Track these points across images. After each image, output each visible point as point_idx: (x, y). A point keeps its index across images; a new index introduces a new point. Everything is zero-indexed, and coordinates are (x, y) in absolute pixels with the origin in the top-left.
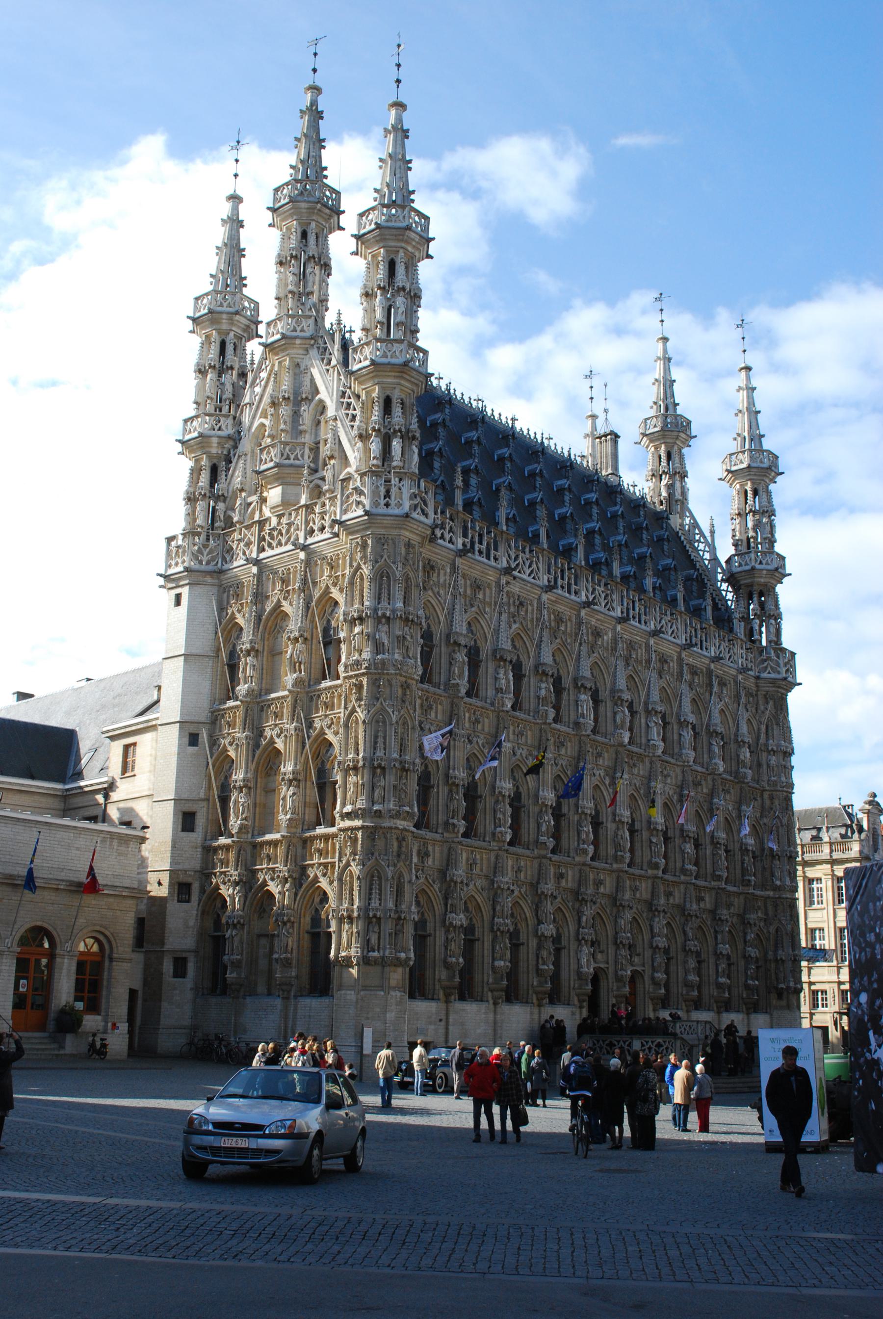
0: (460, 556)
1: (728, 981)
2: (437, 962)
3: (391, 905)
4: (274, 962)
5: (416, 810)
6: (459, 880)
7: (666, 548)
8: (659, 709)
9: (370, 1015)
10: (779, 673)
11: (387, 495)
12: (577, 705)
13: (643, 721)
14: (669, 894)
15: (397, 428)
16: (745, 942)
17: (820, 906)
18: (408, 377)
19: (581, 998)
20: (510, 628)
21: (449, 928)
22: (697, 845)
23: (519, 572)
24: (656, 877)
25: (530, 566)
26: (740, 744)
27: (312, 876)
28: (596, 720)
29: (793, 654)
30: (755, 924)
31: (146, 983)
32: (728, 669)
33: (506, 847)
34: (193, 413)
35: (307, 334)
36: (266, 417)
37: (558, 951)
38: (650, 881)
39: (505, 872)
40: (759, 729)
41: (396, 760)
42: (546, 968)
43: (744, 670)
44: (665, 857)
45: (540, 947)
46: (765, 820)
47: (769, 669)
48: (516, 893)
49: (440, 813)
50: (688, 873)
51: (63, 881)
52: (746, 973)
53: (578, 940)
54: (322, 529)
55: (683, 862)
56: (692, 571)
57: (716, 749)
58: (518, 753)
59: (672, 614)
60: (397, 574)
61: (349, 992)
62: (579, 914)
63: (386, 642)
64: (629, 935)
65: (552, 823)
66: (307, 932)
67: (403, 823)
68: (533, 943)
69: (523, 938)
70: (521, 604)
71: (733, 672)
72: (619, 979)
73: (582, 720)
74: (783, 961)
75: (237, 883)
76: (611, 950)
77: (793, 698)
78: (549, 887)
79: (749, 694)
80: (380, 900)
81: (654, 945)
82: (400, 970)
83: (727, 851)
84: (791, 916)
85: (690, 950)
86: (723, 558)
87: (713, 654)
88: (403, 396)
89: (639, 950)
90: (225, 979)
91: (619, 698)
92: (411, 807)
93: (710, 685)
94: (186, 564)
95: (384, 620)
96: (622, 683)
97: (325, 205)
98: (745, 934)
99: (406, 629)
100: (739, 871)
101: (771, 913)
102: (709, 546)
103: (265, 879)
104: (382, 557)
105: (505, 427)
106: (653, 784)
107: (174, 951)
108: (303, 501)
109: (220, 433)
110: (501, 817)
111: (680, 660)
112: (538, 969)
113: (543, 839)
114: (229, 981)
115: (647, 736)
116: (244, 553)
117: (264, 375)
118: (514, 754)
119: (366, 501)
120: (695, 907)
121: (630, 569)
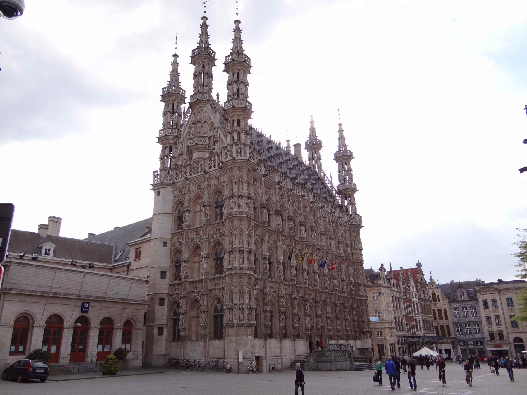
3: (247, 302)
4: (199, 328)
14: (330, 298)
16: (353, 315)
35: (207, 99)
41: (247, 248)
43: (347, 222)
45: (294, 318)
53: (305, 315)
54: (214, 166)
57: (341, 248)
68: (291, 316)
69: (287, 315)
75: (184, 297)
77: (361, 231)
78: (295, 296)
82: (251, 328)
90: (179, 335)
96: (313, 224)
97: (211, 56)
98: (353, 312)
100: (349, 290)
101: (359, 305)
105: (267, 138)
111: (329, 217)
112: (293, 326)
113: (293, 278)
117: (189, 114)
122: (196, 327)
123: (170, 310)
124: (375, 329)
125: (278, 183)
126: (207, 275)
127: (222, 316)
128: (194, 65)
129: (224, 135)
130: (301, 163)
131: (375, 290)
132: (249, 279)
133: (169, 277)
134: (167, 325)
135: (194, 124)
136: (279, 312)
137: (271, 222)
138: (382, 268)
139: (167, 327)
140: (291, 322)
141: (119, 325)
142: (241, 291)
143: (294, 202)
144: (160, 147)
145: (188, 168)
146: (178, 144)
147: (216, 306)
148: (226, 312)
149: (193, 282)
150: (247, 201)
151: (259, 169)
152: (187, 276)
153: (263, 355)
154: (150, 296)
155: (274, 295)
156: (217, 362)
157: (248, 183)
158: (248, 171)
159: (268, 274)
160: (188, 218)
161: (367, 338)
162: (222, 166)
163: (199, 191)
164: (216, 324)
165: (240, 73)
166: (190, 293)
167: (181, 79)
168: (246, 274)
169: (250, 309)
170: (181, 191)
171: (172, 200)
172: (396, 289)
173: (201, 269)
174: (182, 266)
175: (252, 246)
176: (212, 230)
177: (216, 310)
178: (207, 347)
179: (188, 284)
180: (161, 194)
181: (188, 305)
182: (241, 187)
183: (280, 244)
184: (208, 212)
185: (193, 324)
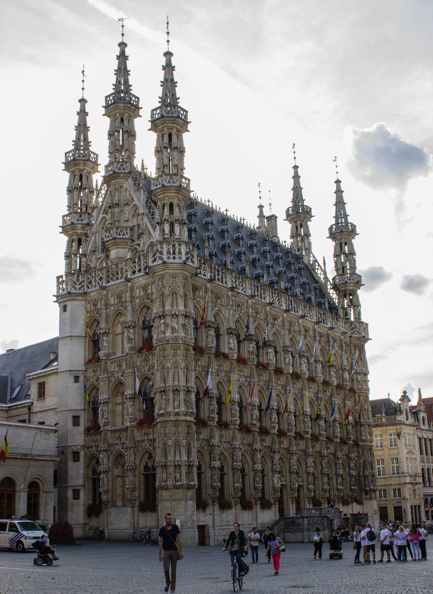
0: (209, 282)
2: (208, 485)
3: (186, 458)
4: (126, 490)
5: (195, 411)
6: (216, 445)
7: (302, 273)
8: (306, 355)
10: (360, 334)
11: (174, 253)
13: (298, 361)
14: (313, 447)
15: (177, 219)
16: (349, 468)
17: (381, 448)
19: (275, 499)
20: (234, 317)
21: (212, 468)
25: (242, 286)
26: (344, 370)
27: (144, 446)
29: (367, 324)
32: (337, 334)
33: (238, 427)
34: (67, 213)
36: (107, 214)
40: (352, 363)
41: (184, 386)
43: (344, 333)
45: (255, 476)
46: (357, 408)
48: (243, 449)
52: (350, 483)
53: (273, 471)
54: (140, 271)
55: (320, 430)
56: (316, 285)
57: (333, 373)
58: (241, 380)
59: (309, 307)
60: (181, 293)
62: (272, 459)
63: (177, 327)
67: (189, 417)
68: (252, 474)
69: (246, 471)
70: (239, 305)
71: (339, 334)
72: (292, 489)
76: (288, 475)
77: (368, 346)
78: (258, 446)
79: (347, 345)
80: (180, 456)
82: (191, 490)
83: (339, 424)
86: (330, 277)
87: (329, 326)
88: (179, 202)
89: (301, 475)
91: (287, 350)
92: (193, 410)
93: (329, 342)
94: (69, 290)
95: (175, 316)
96: (288, 343)
98: (349, 464)
99: (186, 320)
100: (345, 434)
102: (323, 271)
104: (173, 284)
105: (222, 214)
106: (304, 392)
107: (72, 486)
108: (129, 257)
109: (82, 222)
111: (314, 330)
112: (254, 487)
113: (254, 422)
117: (103, 192)
118: (239, 381)
119: (165, 257)
120: (326, 452)
121: (289, 285)
122: (121, 489)
123: (87, 467)
124: (391, 485)
125: (232, 289)
127: (154, 475)
128: (110, 117)
129: (152, 225)
130: (276, 246)
131: (392, 430)
133: (85, 424)
134: (84, 486)
135: (110, 207)
137: (222, 344)
138: (405, 398)
139: (84, 489)
140: (251, 481)
142: (177, 444)
143: (257, 313)
144: (65, 239)
146: (90, 236)
147: (146, 463)
148: (159, 471)
149: (116, 431)
150: (183, 322)
151: (203, 272)
153: (210, 523)
155: (226, 445)
157: (185, 295)
158: (186, 278)
159: (217, 420)
160: (105, 344)
161: (371, 499)
162: (148, 271)
167: (91, 136)
168: (183, 420)
169: (190, 466)
170: (95, 305)
172: (426, 427)
174: (100, 409)
175: (192, 384)
176: (139, 360)
177: (146, 468)
179: (109, 433)
180: (68, 309)
181: (110, 462)
182: (175, 301)
184: (132, 337)
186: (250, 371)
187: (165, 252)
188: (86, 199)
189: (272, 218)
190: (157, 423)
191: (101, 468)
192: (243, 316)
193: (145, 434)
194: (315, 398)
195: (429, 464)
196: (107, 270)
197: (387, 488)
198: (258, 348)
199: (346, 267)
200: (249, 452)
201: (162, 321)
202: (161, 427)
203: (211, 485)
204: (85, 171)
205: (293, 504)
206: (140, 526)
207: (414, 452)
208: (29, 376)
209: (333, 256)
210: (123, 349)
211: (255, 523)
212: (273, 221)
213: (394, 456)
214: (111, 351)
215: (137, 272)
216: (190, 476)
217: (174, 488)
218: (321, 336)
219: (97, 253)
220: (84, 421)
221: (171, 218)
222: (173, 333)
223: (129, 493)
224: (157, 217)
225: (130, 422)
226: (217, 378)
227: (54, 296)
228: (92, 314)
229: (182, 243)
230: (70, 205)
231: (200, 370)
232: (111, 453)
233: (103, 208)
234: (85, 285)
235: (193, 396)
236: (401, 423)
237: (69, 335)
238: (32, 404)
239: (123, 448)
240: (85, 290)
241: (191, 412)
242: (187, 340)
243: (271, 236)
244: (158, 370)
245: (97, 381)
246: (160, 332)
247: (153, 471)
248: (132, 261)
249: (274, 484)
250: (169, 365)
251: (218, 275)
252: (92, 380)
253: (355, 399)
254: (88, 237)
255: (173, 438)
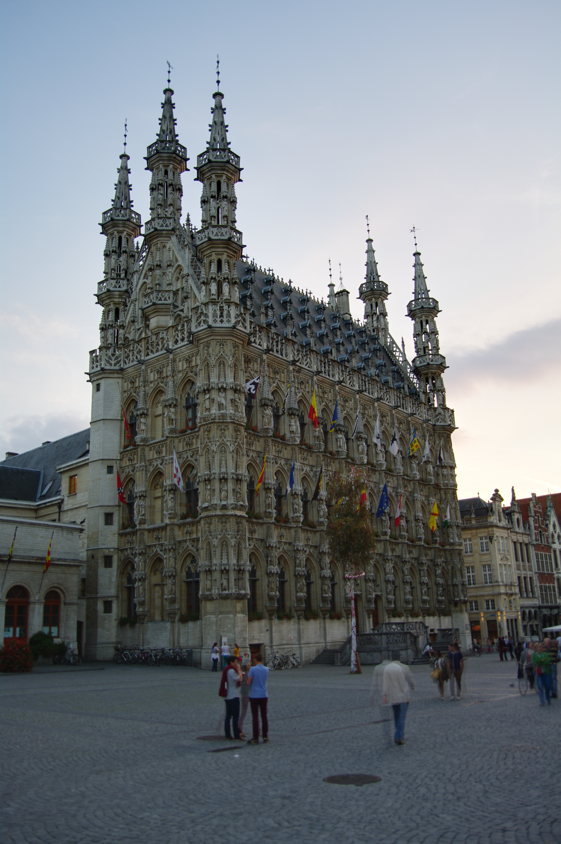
0: (266, 353)
1: (428, 598)
3: (235, 561)
4: (165, 601)
5: (247, 504)
6: (274, 545)
7: (378, 354)
9: (225, 629)
10: (445, 422)
11: (222, 316)
12: (337, 441)
13: (374, 450)
14: (393, 550)
15: (226, 276)
16: (436, 575)
17: (471, 554)
18: (231, 248)
20: (297, 395)
21: (269, 574)
22: (407, 522)
23: (300, 363)
24: (386, 540)
27: (185, 547)
28: (348, 450)
30: (441, 565)
31: (88, 617)
33: (301, 525)
35: (170, 228)
36: (147, 279)
37: (333, 585)
38: (382, 543)
39: (301, 540)
41: (233, 473)
42: (327, 595)
43: (427, 421)
44: (390, 529)
46: (443, 506)
47: (440, 420)
48: (308, 552)
49: (261, 506)
50: (403, 537)
51: (33, 557)
52: (437, 593)
54: (183, 340)
56: (394, 367)
57: (415, 466)
58: (305, 469)
60: (230, 362)
61: (211, 616)
63: (224, 403)
64: (373, 574)
65: (326, 510)
66: (184, 582)
67: (239, 512)
68: (319, 582)
69: (313, 579)
72: (369, 601)
73: (340, 449)
74: (456, 585)
75: (140, 554)
80: (228, 559)
81: (387, 579)
82: (242, 602)
83: (423, 524)
84: (460, 559)
85: (406, 581)
86: (410, 360)
87: (410, 412)
90: (135, 613)
92: (244, 501)
93: (409, 429)
94: (103, 366)
95: (222, 390)
96: (361, 429)
97: (178, 155)
98: (436, 571)
99: (236, 395)
101: (449, 559)
103: (157, 551)
108: (170, 325)
110: (297, 507)
111: (392, 415)
112: (322, 597)
113: (322, 519)
114: (138, 613)
115: (376, 459)
116: (137, 358)
117: (144, 254)
118: (303, 470)
120: (408, 556)
124: (483, 596)
125: (294, 362)
126: (174, 518)
127: (197, 583)
129: (197, 287)
130: (349, 323)
131: (483, 533)
132: (237, 523)
134: (117, 597)
135: (150, 270)
136: (295, 576)
137: (281, 427)
138: (497, 497)
139: (117, 600)
140: (319, 590)
141: (37, 597)
142: (224, 543)
143: (324, 393)
145: (143, 343)
146: (129, 305)
147: (189, 568)
148: (202, 577)
149: (154, 530)
150: (232, 397)
151: (258, 342)
152: (145, 520)
154: (90, 552)
155: (286, 547)
156: (190, 653)
157: (235, 365)
158: (235, 346)
160: (143, 427)
161: (461, 611)
162: (193, 339)
163: (159, 380)
164: (189, 594)
165: (222, 181)
166: (149, 547)
168: (232, 515)
169: (240, 571)
170: (133, 383)
171: (119, 396)
172: (521, 530)
173: (161, 510)
175: (243, 471)
176: (181, 445)
177: (189, 574)
178: (176, 631)
179: (146, 533)
180: (102, 388)
182: (222, 372)
183: (298, 465)
185: (157, 595)
186: (316, 459)
187: (210, 315)
188: (125, 264)
189: (344, 293)
190: (201, 518)
191: (136, 575)
192: (307, 395)
193: (187, 533)
194: (394, 494)
195: (525, 572)
196: (146, 341)
197: (478, 599)
198: (326, 433)
199: (428, 347)
200: (315, 556)
201: (207, 396)
202: (205, 524)
203: (268, 595)
204: (125, 233)
205: (369, 618)
206: (181, 645)
207: (509, 557)
208: (60, 469)
209: (412, 336)
210: (163, 431)
211: (323, 641)
212: (345, 297)
213: (486, 563)
214: (150, 436)
215: (179, 341)
216: (240, 583)
217: (221, 598)
218: (400, 423)
219: (136, 324)
220: (119, 519)
221: (218, 277)
222: (219, 410)
223: (168, 604)
224: (202, 276)
225: (169, 518)
226: (276, 466)
227: (86, 373)
228: (129, 393)
229: (231, 304)
230: (107, 271)
231: (254, 456)
232: (149, 557)
233: (144, 272)
234: (122, 360)
235: (245, 487)
236: (492, 526)
237: (102, 418)
238: (63, 501)
239: (161, 551)
240: (122, 366)
241: (242, 505)
242: (236, 418)
243: (342, 313)
244: (202, 455)
245: (133, 471)
246: (204, 409)
247: (196, 577)
248: (175, 329)
249: (346, 594)
250: (214, 448)
251: (277, 346)
252: (127, 470)
253: (441, 496)
254: (127, 306)
255: (220, 537)
